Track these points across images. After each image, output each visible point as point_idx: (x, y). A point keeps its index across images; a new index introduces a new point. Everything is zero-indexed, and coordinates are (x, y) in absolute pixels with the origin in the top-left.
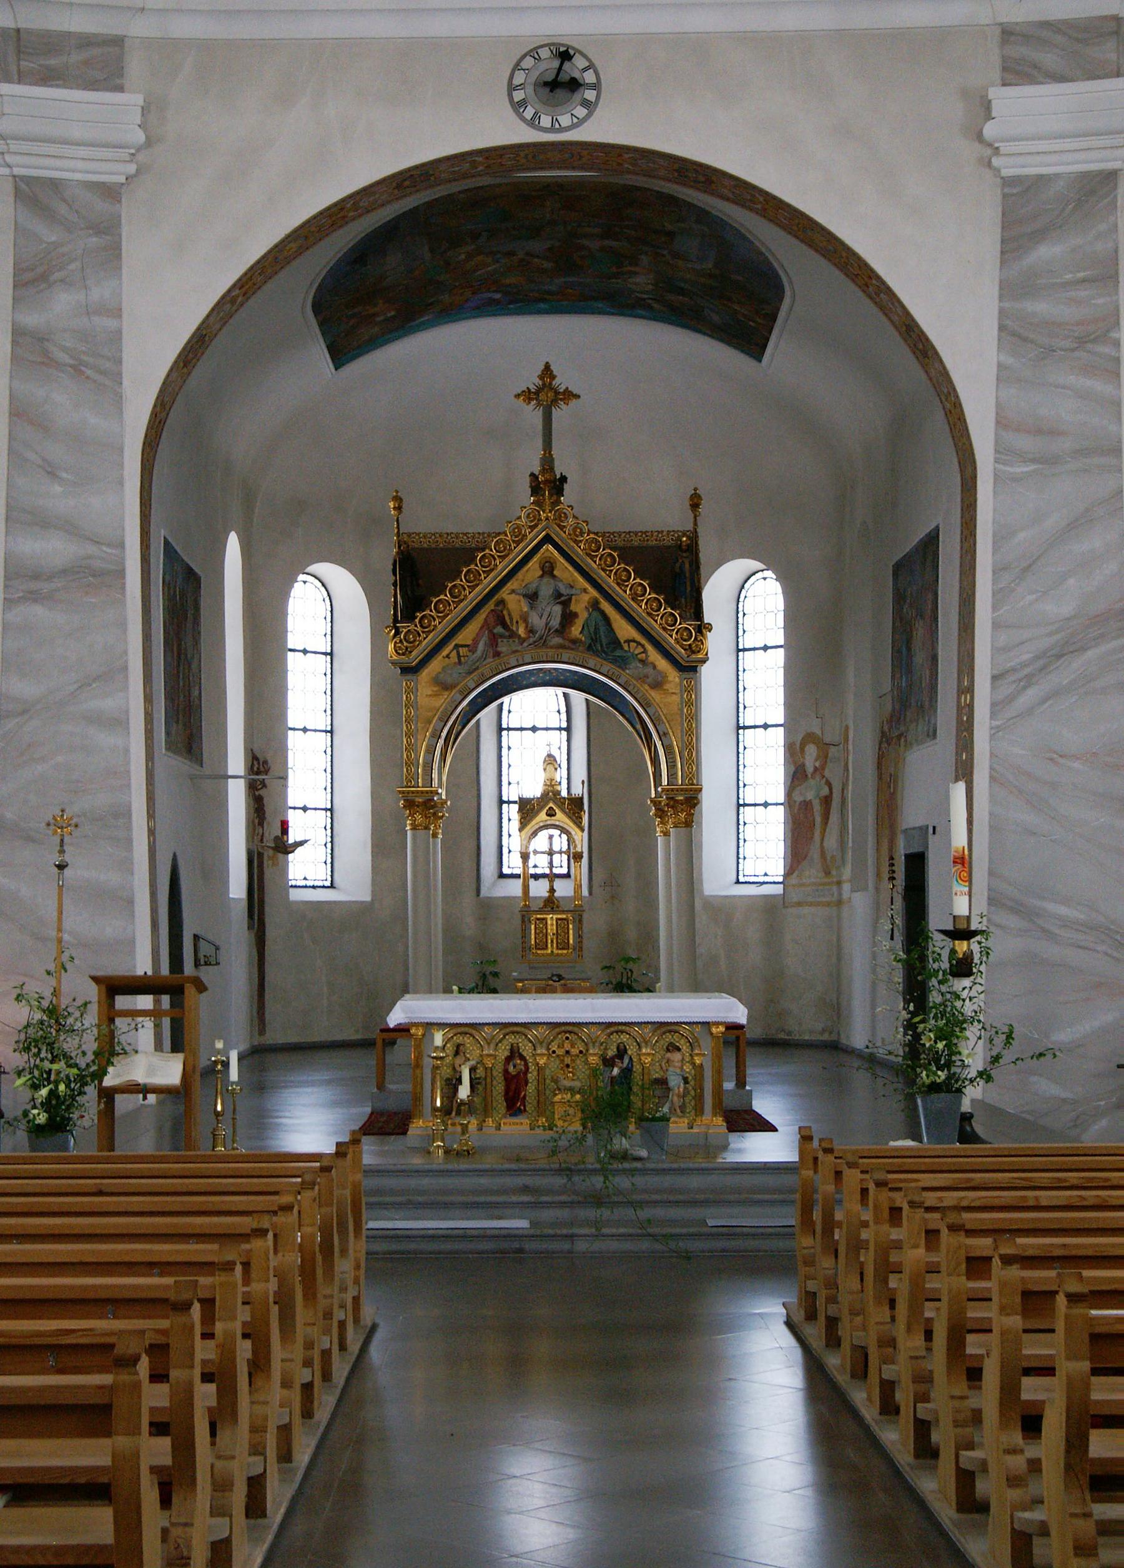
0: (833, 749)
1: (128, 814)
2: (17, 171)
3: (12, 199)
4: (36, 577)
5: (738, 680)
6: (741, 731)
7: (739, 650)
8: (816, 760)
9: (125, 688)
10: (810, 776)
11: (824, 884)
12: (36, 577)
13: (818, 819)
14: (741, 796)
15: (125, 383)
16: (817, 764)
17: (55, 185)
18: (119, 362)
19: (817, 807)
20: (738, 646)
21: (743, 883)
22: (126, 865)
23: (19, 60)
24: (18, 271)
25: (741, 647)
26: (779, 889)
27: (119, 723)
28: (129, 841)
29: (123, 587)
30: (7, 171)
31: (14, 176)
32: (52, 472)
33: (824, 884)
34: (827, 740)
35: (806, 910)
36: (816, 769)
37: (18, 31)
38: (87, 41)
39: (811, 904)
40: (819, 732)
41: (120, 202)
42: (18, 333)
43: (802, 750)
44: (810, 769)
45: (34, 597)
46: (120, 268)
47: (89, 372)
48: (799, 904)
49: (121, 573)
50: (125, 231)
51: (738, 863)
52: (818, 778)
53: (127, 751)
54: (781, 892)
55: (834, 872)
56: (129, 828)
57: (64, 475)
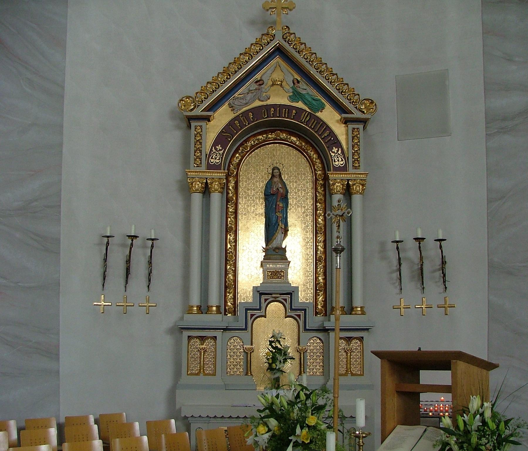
4: (504, 119)
57: (517, 59)
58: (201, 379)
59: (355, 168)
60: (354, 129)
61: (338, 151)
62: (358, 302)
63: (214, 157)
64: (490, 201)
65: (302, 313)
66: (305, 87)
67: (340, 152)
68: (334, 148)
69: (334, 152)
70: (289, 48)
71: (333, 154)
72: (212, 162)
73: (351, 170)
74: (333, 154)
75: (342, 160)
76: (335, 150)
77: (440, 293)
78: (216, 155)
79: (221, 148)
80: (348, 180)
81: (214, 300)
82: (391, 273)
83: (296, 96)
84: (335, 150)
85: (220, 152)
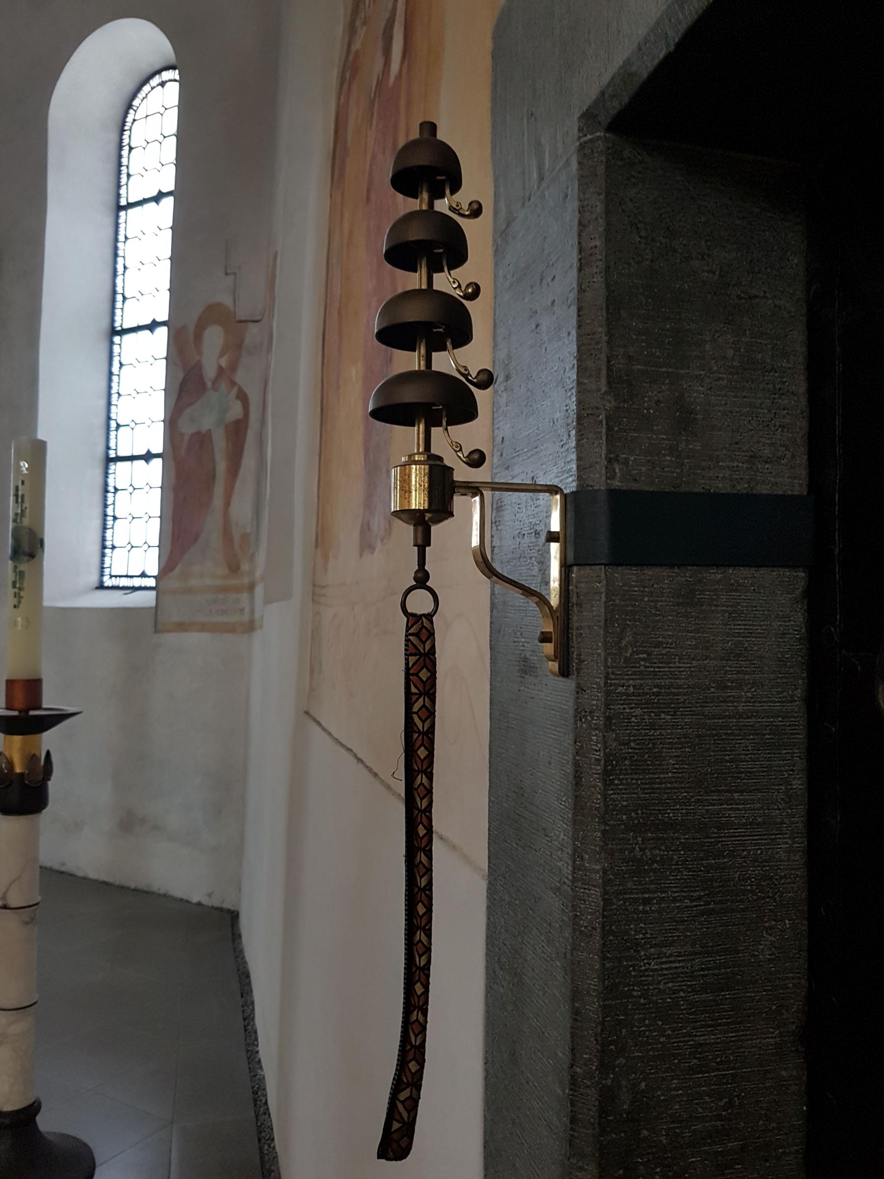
0: (253, 329)
5: (116, 255)
6: (117, 339)
7: (120, 208)
8: (222, 355)
10: (209, 384)
11: (225, 589)
13: (221, 466)
14: (112, 444)
16: (223, 362)
19: (220, 443)
20: (118, 201)
21: (108, 588)
25: (123, 202)
26: (147, 599)
33: (225, 589)
34: (241, 315)
35: (193, 638)
36: (220, 369)
39: (203, 627)
40: (227, 301)
43: (198, 337)
44: (210, 373)
48: (182, 627)
51: (103, 555)
52: (223, 386)
54: (153, 604)
55: (245, 567)
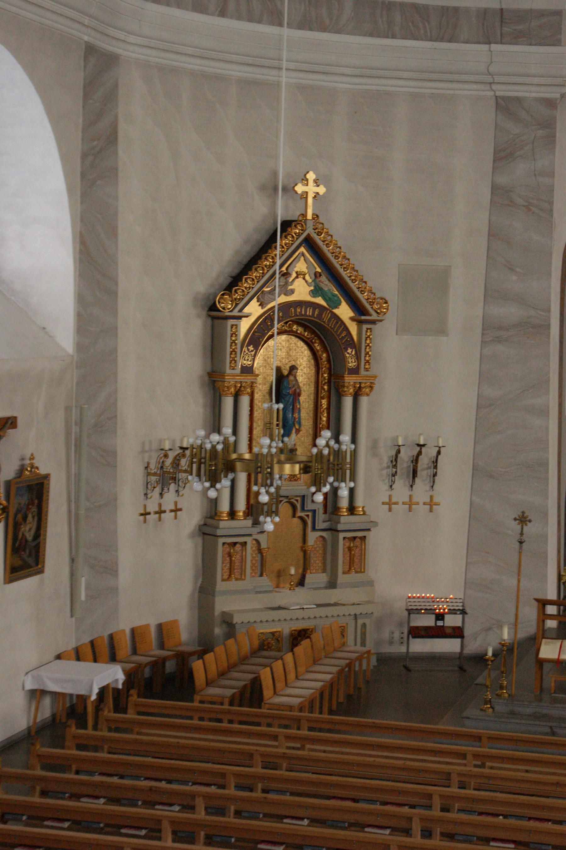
1: (546, 464)
2: (498, 94)
3: (494, 109)
4: (500, 328)
9: (548, 393)
12: (500, 328)
15: (555, 215)
17: (519, 100)
18: (551, 203)
22: (545, 493)
23: (502, 26)
24: (496, 152)
27: (544, 412)
28: (547, 479)
29: (549, 335)
30: (492, 93)
31: (496, 97)
32: (511, 268)
37: (502, 9)
38: (541, 14)
41: (556, 109)
42: (495, 188)
45: (498, 340)
46: (555, 148)
47: (534, 209)
49: (548, 326)
50: (558, 126)
53: (547, 428)
56: (547, 472)
57: (518, 269)
58: (233, 585)
59: (367, 370)
60: (367, 329)
61: (352, 352)
62: (359, 502)
63: (246, 359)
64: (478, 408)
65: (310, 514)
66: (327, 282)
67: (353, 353)
68: (349, 349)
69: (348, 353)
70: (317, 239)
71: (348, 355)
72: (245, 364)
73: (362, 372)
74: (348, 355)
75: (355, 362)
76: (349, 351)
77: (427, 491)
78: (248, 357)
79: (252, 349)
80: (360, 383)
81: (241, 505)
82: (382, 469)
83: (317, 291)
84: (349, 351)
85: (252, 353)
